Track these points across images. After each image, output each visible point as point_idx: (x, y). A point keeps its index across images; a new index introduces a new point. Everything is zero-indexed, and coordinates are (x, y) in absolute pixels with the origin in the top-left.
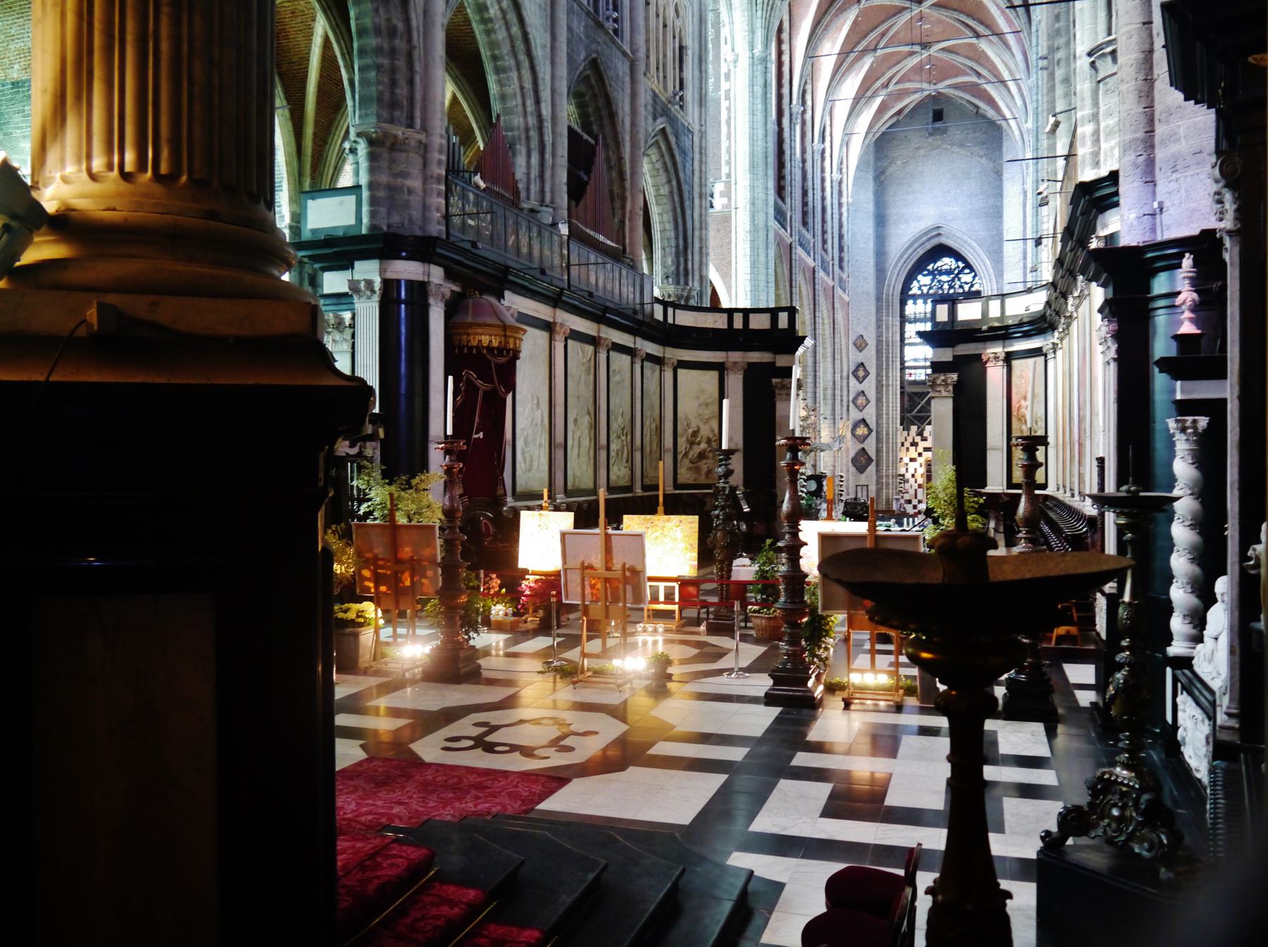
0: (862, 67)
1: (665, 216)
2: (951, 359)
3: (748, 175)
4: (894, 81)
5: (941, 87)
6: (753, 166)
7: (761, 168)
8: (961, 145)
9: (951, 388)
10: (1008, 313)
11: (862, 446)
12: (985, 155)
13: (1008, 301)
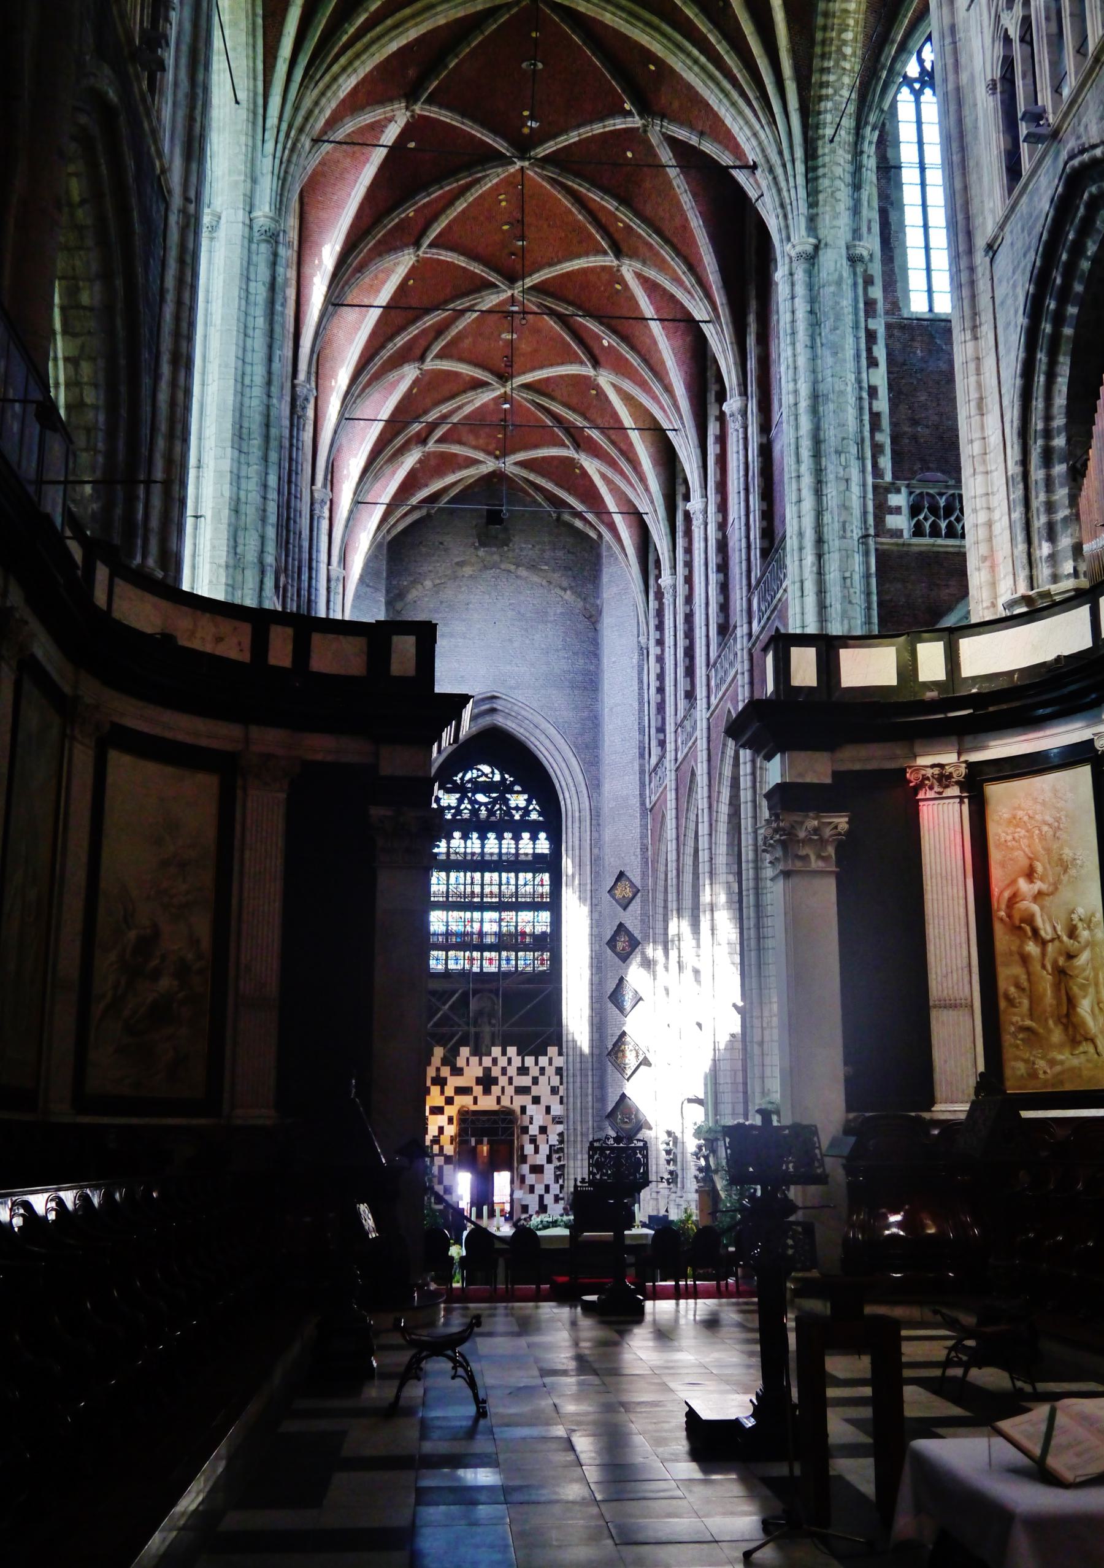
0: (394, 385)
1: (86, 368)
3: (229, 450)
4: (438, 433)
5: (509, 465)
6: (240, 435)
7: (257, 442)
8: (533, 567)
9: (831, 850)
10: (968, 670)
12: (571, 588)
13: (967, 646)
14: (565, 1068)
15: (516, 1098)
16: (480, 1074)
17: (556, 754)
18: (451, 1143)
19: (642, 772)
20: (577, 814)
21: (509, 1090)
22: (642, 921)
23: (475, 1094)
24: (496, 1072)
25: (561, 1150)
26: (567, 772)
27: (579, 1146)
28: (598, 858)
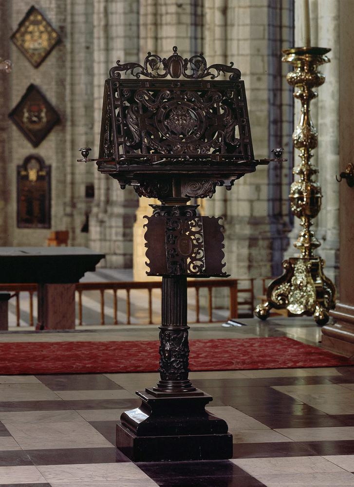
2: (147, 249)
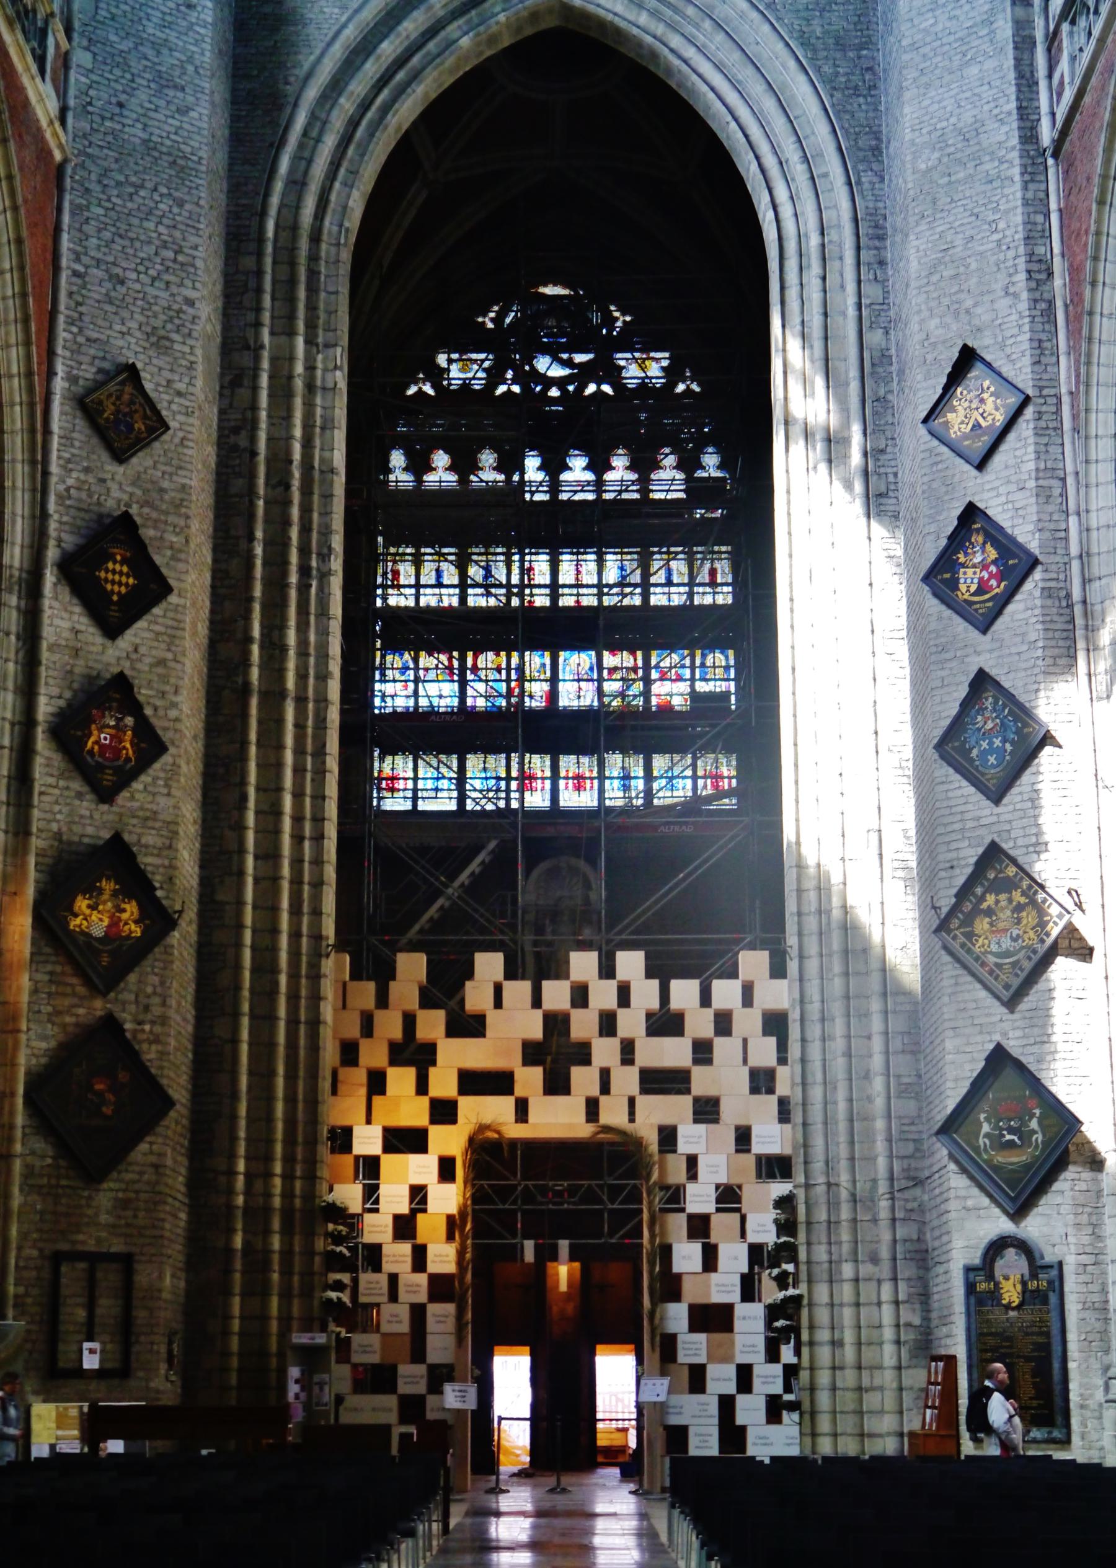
11: (99, 1006)
14: (794, 1016)
15: (642, 1101)
16: (536, 1032)
17: (746, 74)
18: (450, 1237)
19: (1023, 44)
20: (814, 240)
21: (627, 1081)
22: (1043, 494)
23: (519, 1091)
24: (583, 1025)
25: (787, 1252)
26: (779, 123)
27: (845, 1236)
28: (884, 357)
